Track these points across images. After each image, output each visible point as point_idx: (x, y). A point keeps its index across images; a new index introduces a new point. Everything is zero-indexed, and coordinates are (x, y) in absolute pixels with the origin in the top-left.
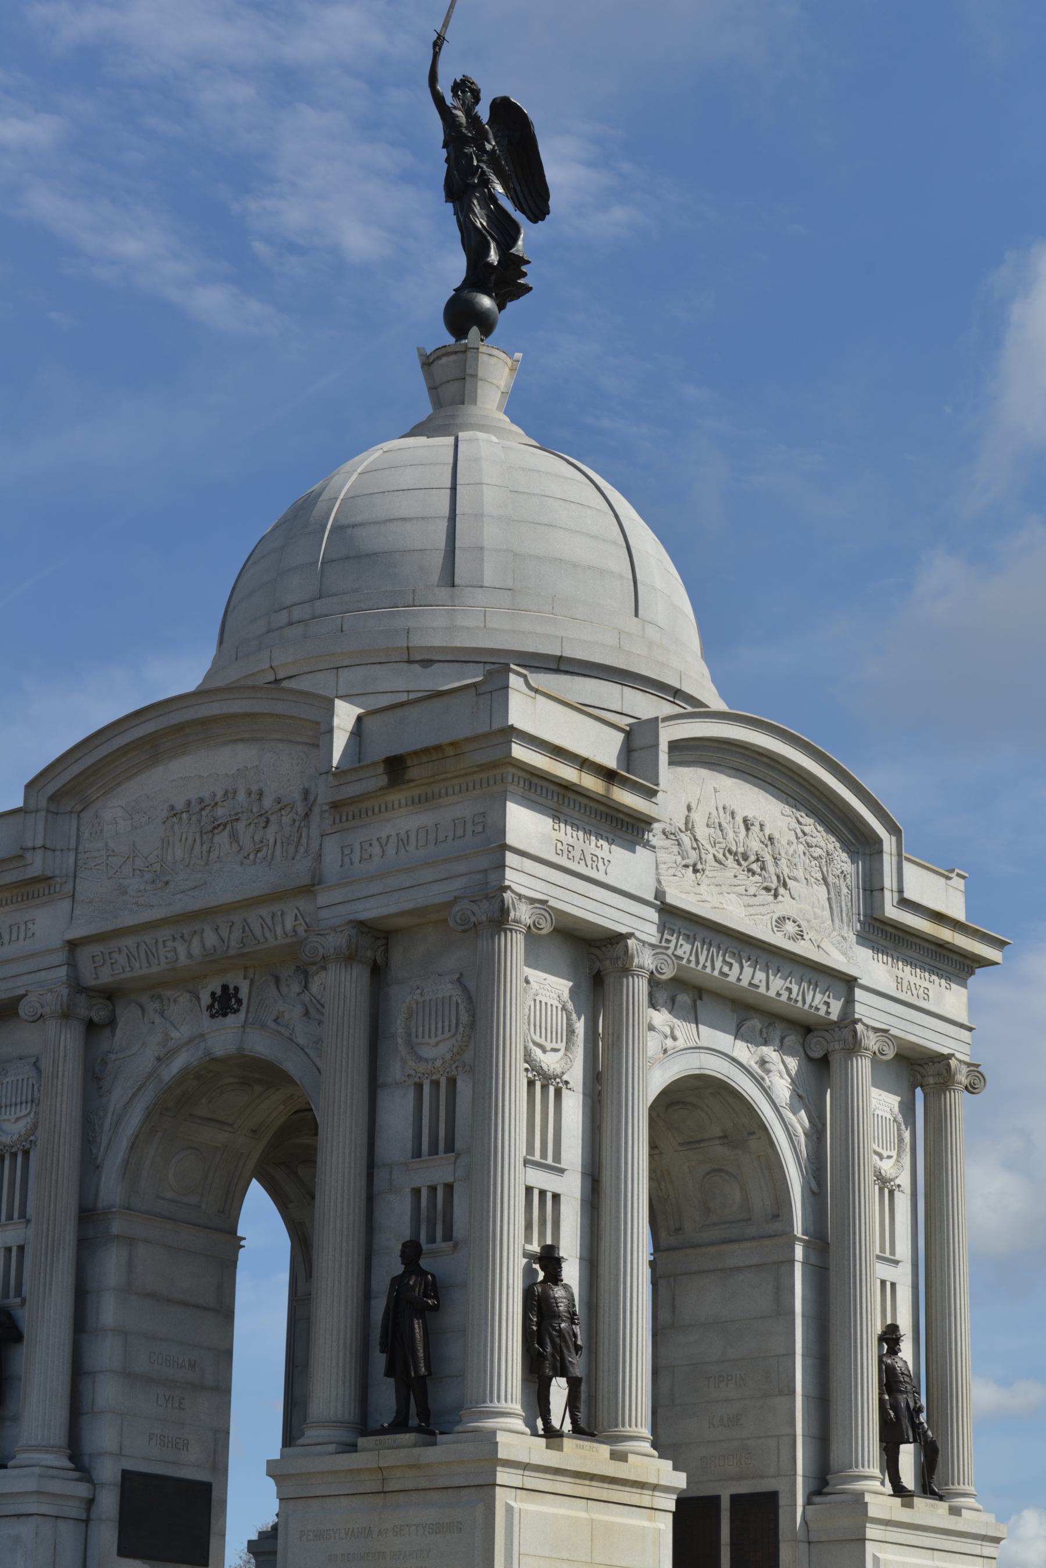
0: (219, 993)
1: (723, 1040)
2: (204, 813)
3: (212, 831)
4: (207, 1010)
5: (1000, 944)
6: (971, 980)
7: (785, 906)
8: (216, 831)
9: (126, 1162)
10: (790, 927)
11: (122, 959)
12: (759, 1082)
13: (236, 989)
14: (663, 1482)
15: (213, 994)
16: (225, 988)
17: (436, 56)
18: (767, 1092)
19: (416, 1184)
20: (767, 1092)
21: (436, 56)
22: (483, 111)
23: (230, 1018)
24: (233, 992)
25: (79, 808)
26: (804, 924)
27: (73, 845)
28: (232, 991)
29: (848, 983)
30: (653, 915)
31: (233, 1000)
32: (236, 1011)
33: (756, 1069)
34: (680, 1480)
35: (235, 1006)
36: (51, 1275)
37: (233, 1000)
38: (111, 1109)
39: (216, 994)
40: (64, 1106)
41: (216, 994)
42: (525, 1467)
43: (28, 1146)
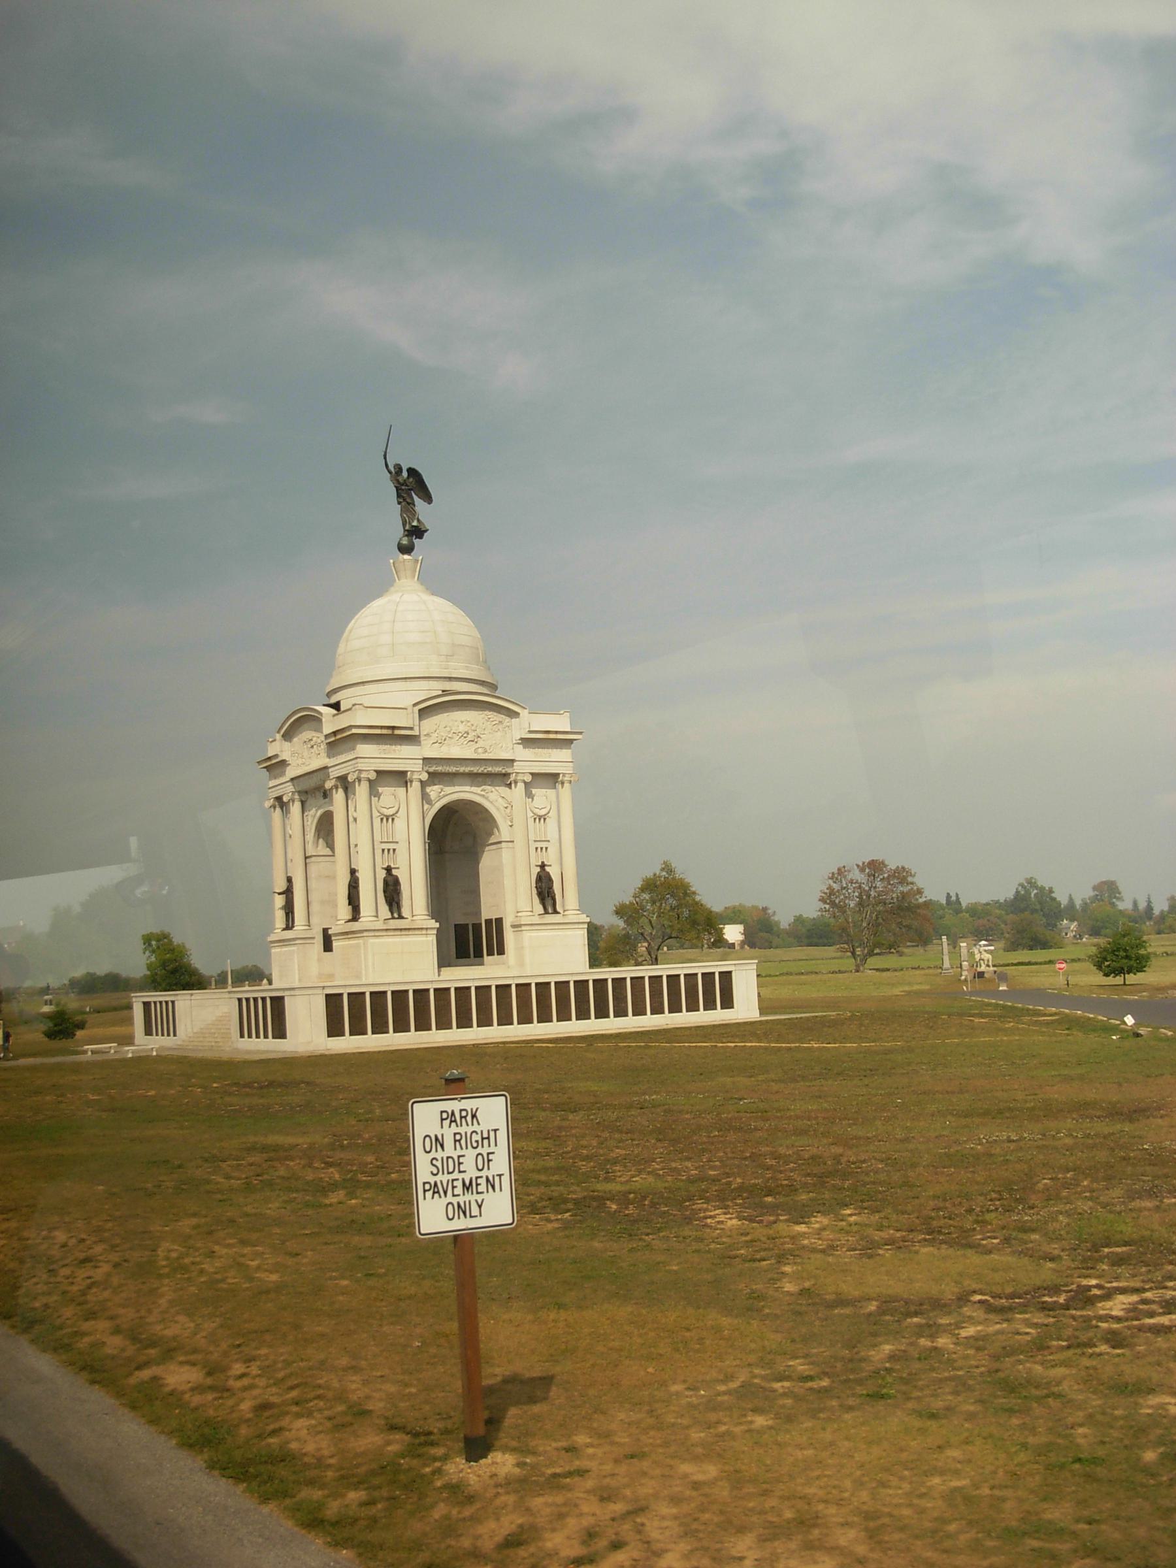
1: (467, 788)
5: (581, 733)
6: (572, 746)
7: (481, 743)
10: (480, 750)
12: (483, 796)
14: (429, 927)
17: (385, 458)
18: (487, 798)
20: (487, 798)
21: (385, 458)
22: (405, 474)
26: (488, 748)
29: (513, 761)
30: (421, 761)
33: (483, 793)
34: (437, 925)
42: (374, 930)
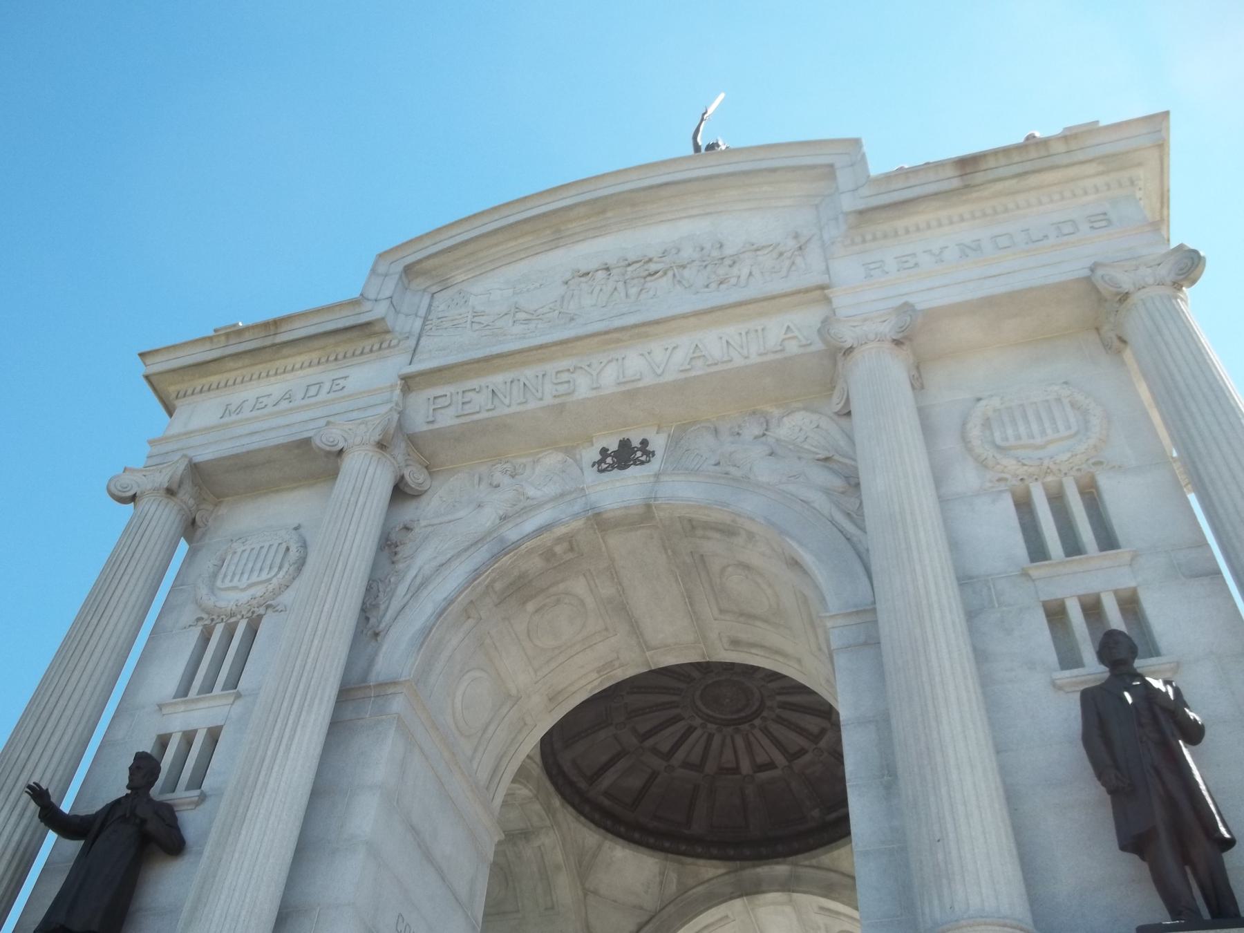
0: (613, 447)
2: (630, 269)
3: (645, 278)
4: (593, 466)
8: (649, 279)
9: (426, 632)
11: (481, 400)
13: (645, 443)
15: (604, 452)
16: (625, 444)
19: (1054, 592)
23: (633, 470)
24: (639, 446)
25: (434, 289)
27: (422, 312)
28: (636, 443)
31: (639, 454)
32: (642, 463)
35: (643, 458)
36: (294, 730)
37: (639, 454)
38: (412, 573)
39: (608, 450)
40: (358, 537)
41: (608, 450)
43: (262, 611)
